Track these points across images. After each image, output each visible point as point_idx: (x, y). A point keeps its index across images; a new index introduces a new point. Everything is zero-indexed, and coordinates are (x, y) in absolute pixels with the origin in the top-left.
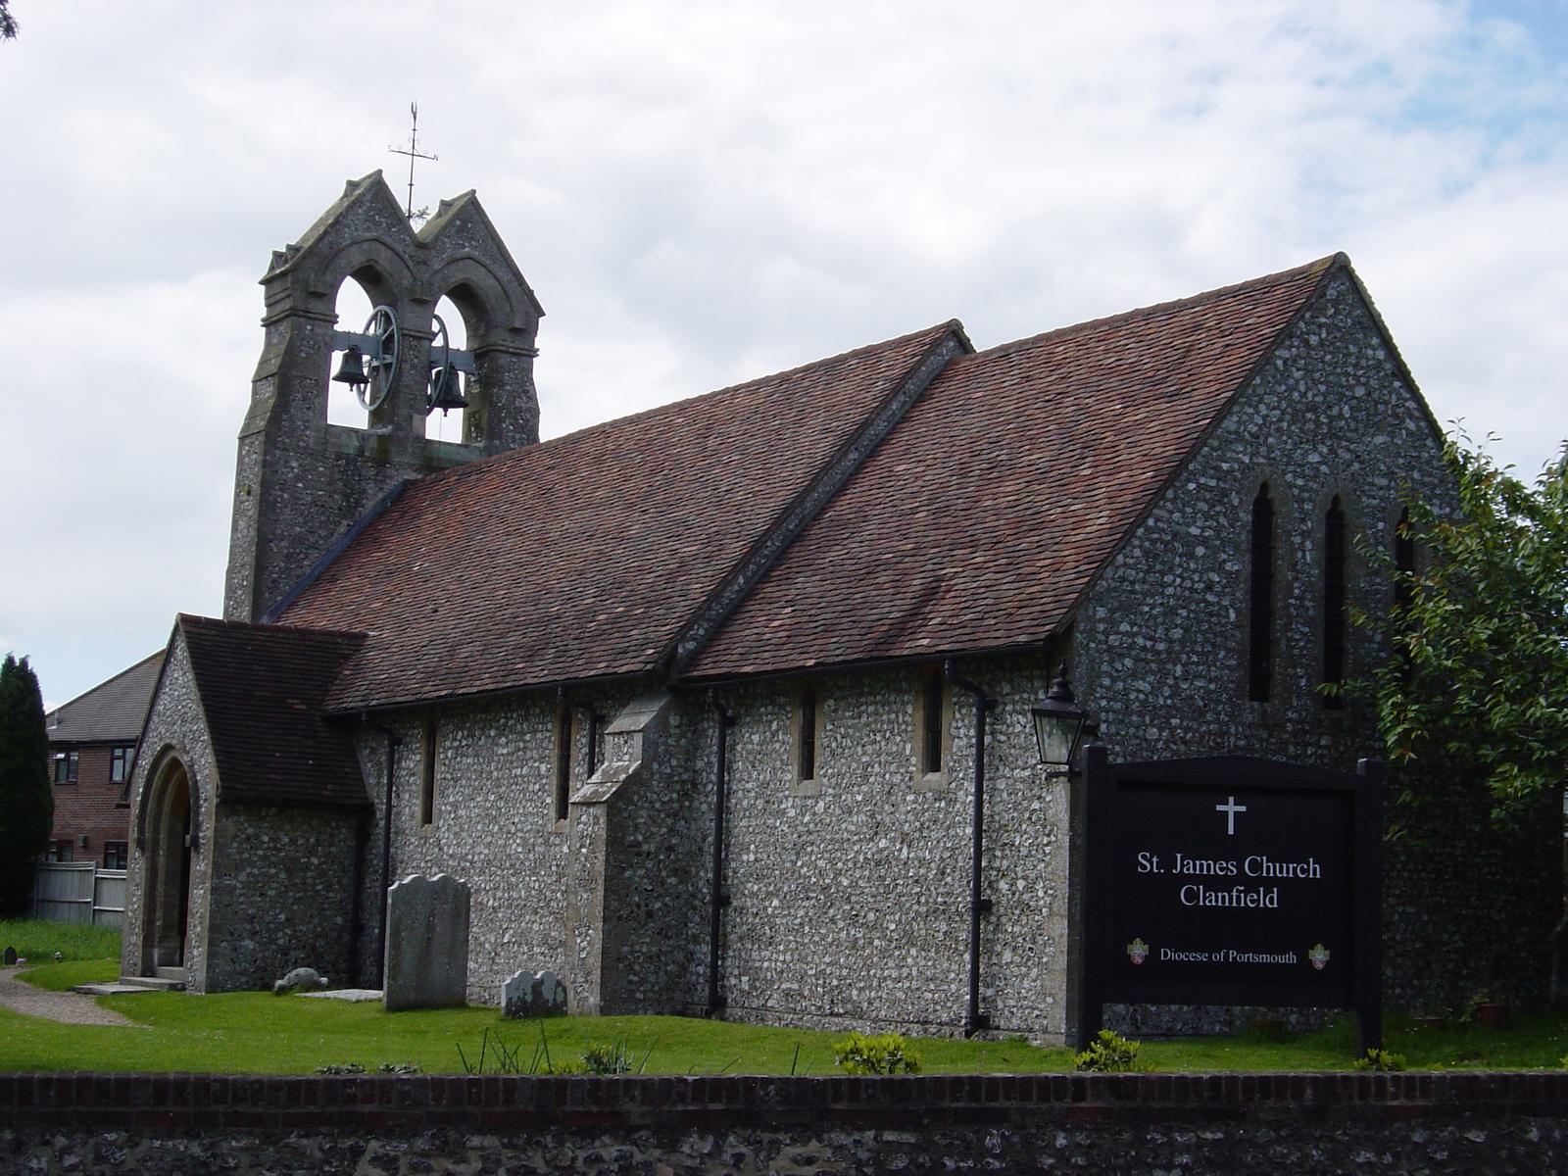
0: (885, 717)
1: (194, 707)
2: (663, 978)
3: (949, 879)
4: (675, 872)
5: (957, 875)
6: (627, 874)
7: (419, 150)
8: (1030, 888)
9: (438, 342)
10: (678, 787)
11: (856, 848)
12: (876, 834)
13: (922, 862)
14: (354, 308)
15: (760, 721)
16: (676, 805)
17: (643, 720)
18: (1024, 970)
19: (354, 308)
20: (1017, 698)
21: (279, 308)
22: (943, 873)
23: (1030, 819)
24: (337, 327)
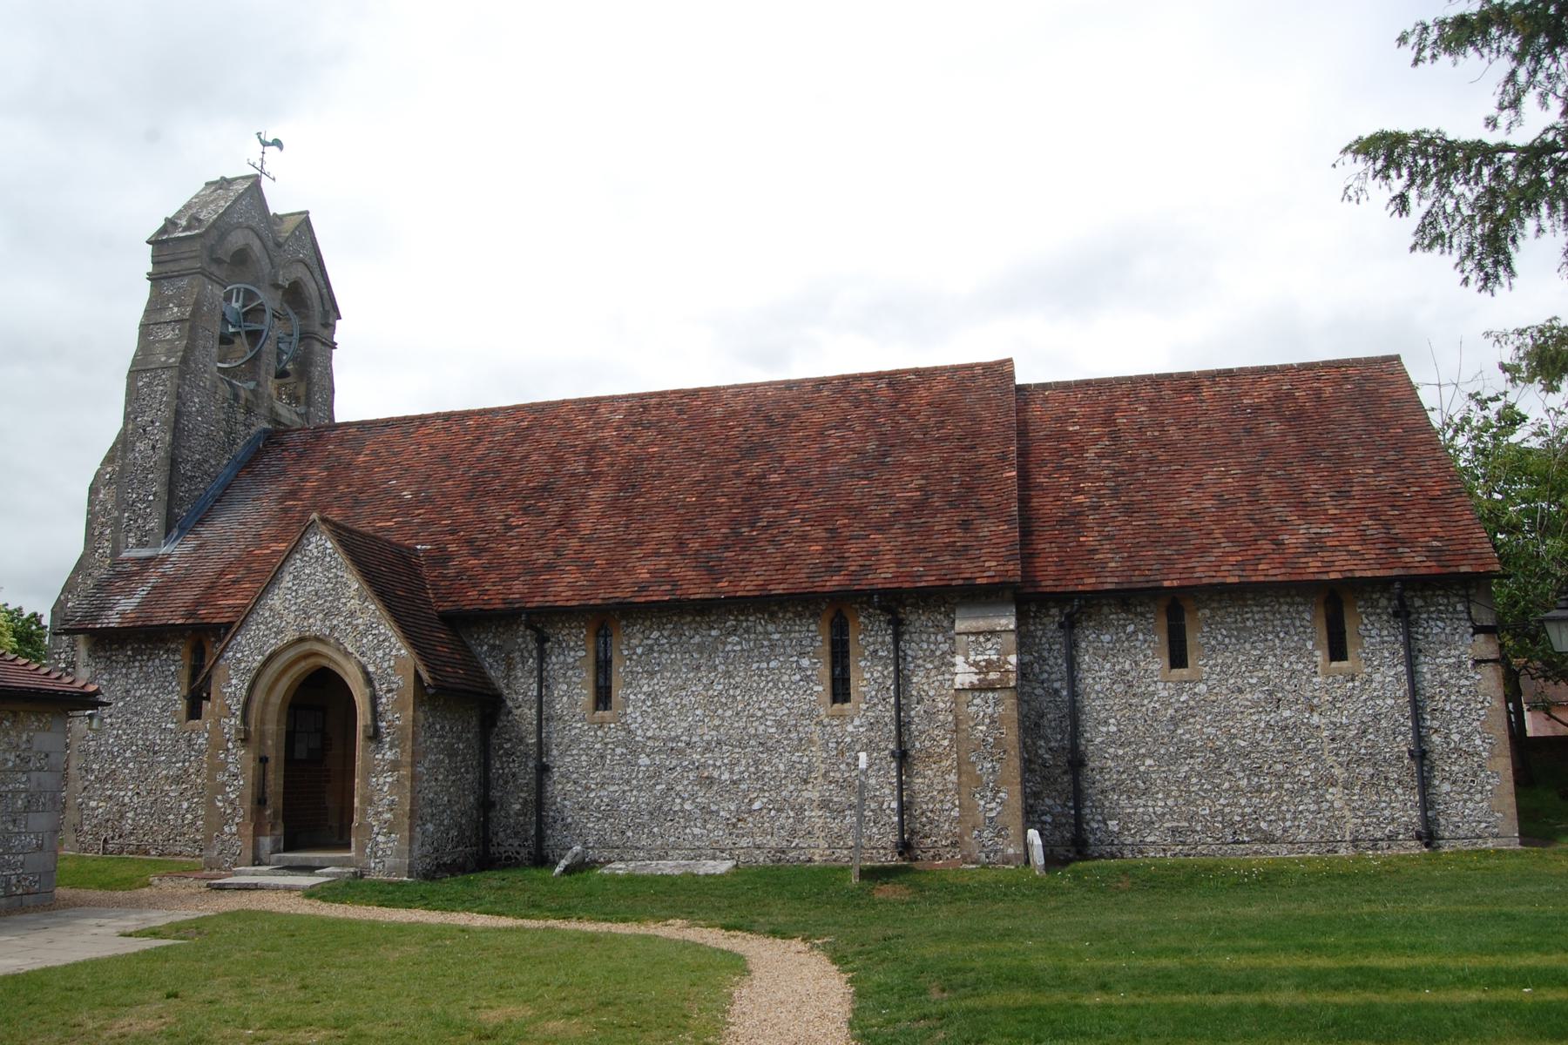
8: (1469, 737)
11: (1254, 718)
18: (1466, 796)
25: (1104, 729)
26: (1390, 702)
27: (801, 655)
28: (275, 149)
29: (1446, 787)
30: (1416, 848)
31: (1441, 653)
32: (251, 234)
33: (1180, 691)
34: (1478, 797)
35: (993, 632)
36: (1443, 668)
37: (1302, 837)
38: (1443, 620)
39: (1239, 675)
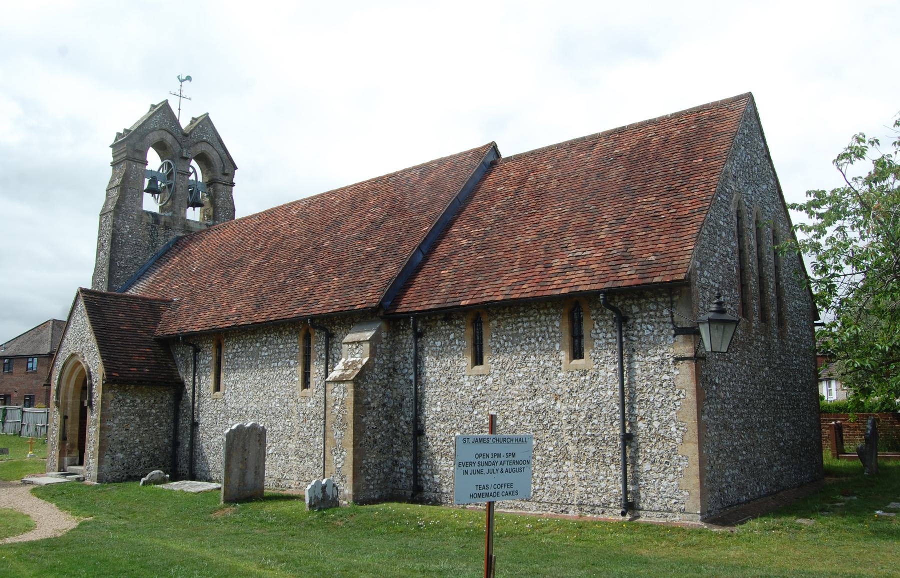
0: (538, 329)
1: (89, 335)
2: (382, 476)
3: (595, 421)
4: (386, 417)
5: (602, 419)
6: (364, 420)
7: (183, 94)
8: (666, 425)
9: (192, 177)
10: (386, 371)
11: (520, 403)
12: (535, 395)
13: (573, 412)
14: (154, 161)
15: (441, 334)
16: (386, 381)
17: (368, 335)
18: (661, 475)
19: (154, 161)
20: (645, 315)
21: (119, 158)
22: (591, 417)
23: (661, 385)
24: (148, 168)
25: (434, 409)
26: (610, 393)
27: (291, 358)
28: (188, 81)
29: (647, 466)
30: (615, 515)
31: (650, 352)
32: (164, 132)
33: (477, 383)
34: (671, 477)
35: (359, 342)
36: (650, 366)
37: (545, 498)
38: (651, 323)
39: (512, 370)
